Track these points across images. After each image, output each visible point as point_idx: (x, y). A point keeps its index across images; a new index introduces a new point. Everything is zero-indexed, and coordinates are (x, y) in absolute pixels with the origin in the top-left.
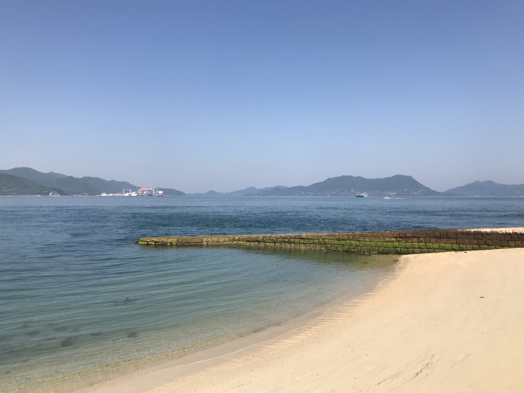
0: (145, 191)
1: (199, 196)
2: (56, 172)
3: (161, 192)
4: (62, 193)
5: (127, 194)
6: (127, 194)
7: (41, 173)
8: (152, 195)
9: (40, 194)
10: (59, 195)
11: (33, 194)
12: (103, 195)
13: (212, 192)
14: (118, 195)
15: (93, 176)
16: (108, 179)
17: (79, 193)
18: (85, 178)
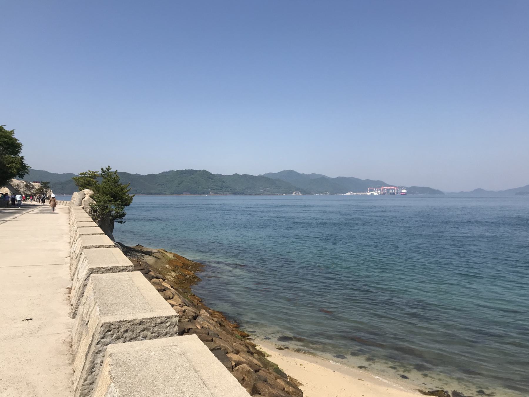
0: (390, 189)
1: (462, 195)
2: (317, 173)
3: (404, 191)
4: (304, 192)
5: (369, 194)
6: (369, 194)
7: (164, 174)
8: (394, 194)
9: (286, 193)
10: (301, 194)
11: (280, 193)
12: (349, 194)
13: (479, 191)
14: (361, 193)
15: (347, 176)
16: (363, 178)
17: (322, 193)
18: (339, 179)
